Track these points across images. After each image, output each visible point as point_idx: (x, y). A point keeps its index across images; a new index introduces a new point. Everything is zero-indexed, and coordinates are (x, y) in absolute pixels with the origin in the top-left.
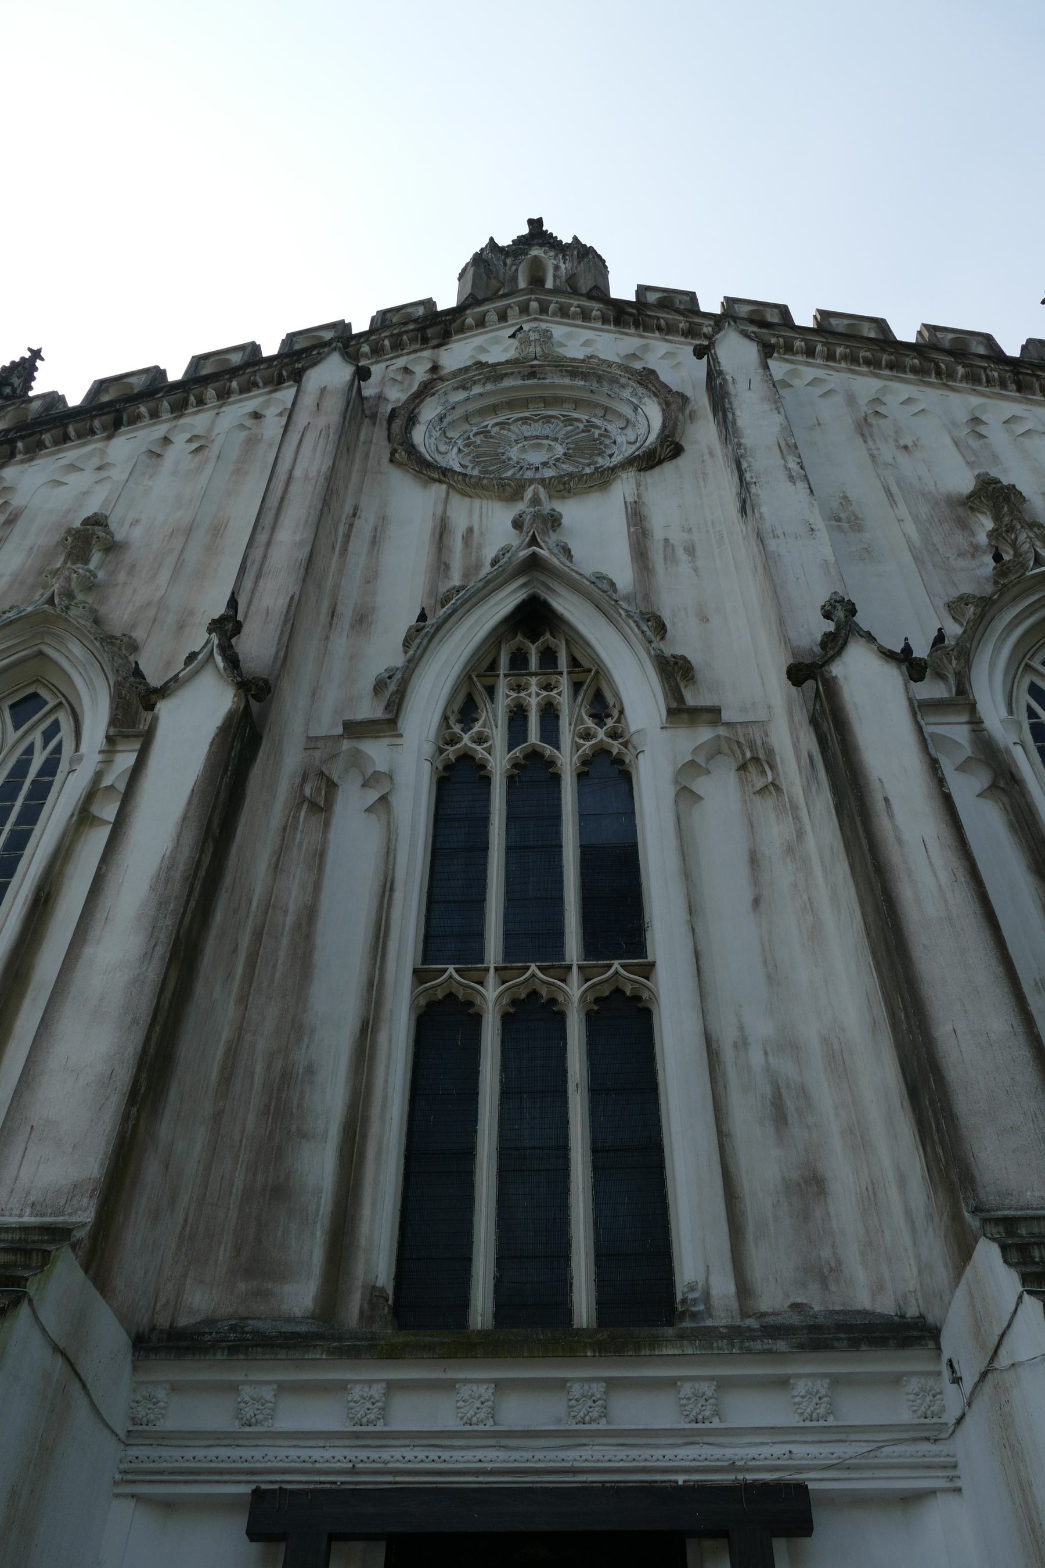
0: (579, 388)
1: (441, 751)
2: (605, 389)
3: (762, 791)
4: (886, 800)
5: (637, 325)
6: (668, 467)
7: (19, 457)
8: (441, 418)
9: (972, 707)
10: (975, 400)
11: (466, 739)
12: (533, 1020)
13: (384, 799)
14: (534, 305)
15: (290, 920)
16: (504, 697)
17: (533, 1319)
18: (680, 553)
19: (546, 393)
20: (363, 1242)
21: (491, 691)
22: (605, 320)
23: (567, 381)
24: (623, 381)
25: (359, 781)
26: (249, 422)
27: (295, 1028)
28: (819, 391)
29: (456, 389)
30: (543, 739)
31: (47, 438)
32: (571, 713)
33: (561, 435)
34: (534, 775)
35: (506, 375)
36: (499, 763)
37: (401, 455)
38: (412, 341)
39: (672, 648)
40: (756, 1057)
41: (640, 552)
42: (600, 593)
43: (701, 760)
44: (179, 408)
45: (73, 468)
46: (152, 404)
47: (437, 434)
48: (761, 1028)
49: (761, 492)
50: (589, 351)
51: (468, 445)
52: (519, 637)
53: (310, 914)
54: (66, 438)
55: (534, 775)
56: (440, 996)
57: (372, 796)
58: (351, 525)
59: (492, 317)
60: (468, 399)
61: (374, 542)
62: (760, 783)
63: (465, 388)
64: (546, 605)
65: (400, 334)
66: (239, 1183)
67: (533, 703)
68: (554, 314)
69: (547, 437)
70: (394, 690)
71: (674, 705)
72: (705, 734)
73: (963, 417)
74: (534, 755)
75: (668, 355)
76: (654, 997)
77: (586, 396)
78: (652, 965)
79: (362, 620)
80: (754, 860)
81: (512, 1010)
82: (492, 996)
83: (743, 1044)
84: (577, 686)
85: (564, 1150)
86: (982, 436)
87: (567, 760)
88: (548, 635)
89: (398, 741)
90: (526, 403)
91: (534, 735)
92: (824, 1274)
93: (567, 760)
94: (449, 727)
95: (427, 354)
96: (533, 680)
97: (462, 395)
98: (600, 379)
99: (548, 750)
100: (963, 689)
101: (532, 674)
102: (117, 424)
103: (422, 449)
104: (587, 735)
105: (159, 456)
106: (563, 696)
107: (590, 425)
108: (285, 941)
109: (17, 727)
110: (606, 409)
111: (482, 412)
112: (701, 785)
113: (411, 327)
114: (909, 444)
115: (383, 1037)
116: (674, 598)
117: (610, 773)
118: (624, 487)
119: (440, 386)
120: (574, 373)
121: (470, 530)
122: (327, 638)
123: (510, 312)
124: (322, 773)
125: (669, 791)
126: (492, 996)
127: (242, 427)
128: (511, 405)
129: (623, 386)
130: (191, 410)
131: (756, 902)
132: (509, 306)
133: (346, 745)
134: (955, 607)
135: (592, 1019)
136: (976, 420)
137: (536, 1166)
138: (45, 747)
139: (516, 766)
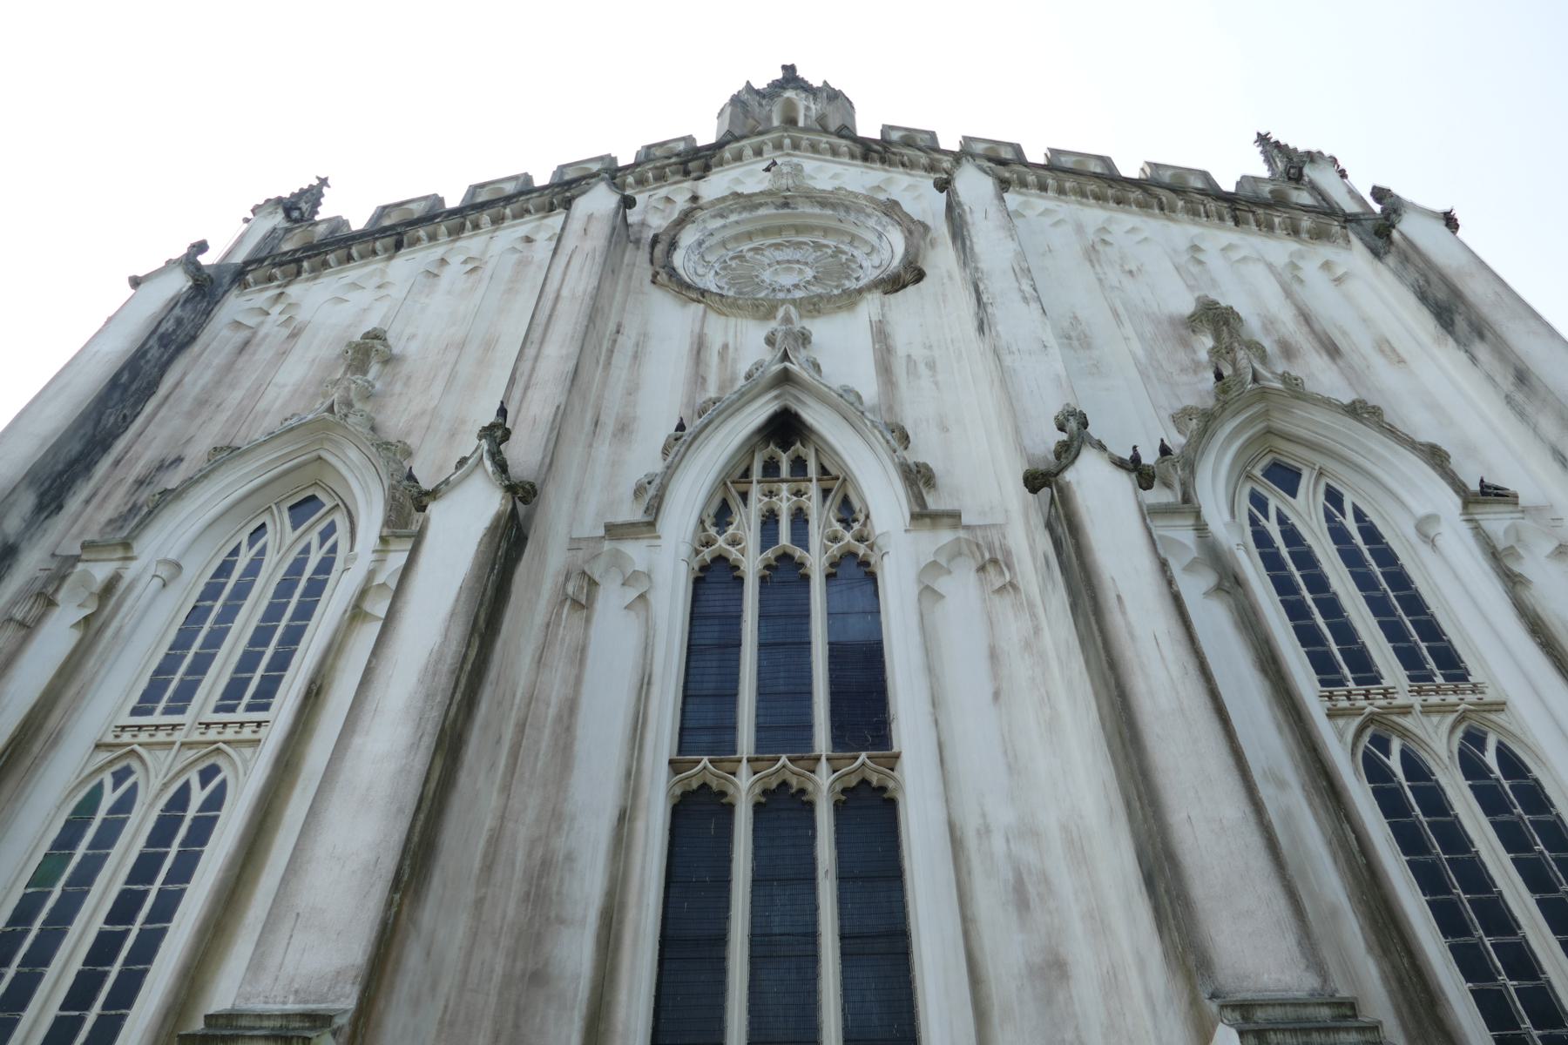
0: (829, 217)
1: (697, 553)
2: (852, 217)
3: (1002, 589)
4: (1119, 597)
5: (883, 161)
6: (911, 289)
7: (304, 276)
8: (700, 244)
9: (1198, 514)
11: (721, 541)
12: (783, 809)
13: (642, 597)
14: (787, 142)
15: (552, 712)
18: (922, 368)
19: (798, 221)
20: (620, 1027)
21: (744, 496)
22: (853, 157)
23: (817, 210)
24: (868, 210)
25: (619, 581)
26: (520, 246)
27: (555, 817)
28: (1048, 221)
29: (714, 217)
30: (793, 541)
31: (331, 258)
32: (819, 519)
33: (810, 260)
34: (785, 575)
35: (761, 205)
36: (752, 564)
37: (663, 277)
38: (674, 173)
39: (916, 455)
40: (998, 844)
41: (885, 369)
42: (847, 405)
43: (943, 561)
44: (456, 232)
45: (355, 286)
46: (430, 228)
47: (695, 258)
48: (1003, 816)
49: (997, 313)
50: (837, 183)
51: (724, 268)
52: (772, 446)
53: (571, 707)
54: (350, 258)
55: (785, 575)
56: (695, 785)
57: (632, 594)
58: (615, 341)
59: (748, 152)
60: (724, 226)
61: (635, 356)
62: (998, 583)
63: (722, 216)
64: (796, 416)
65: (663, 167)
66: (499, 970)
67: (784, 507)
68: (806, 150)
69: (798, 262)
70: (653, 497)
71: (917, 509)
72: (946, 536)
73: (1183, 244)
74: (785, 557)
75: (910, 187)
76: (900, 786)
77: (834, 224)
78: (897, 756)
79: (624, 429)
80: (994, 656)
81: (763, 800)
83: (985, 831)
84: (826, 492)
85: (812, 936)
86: (1200, 262)
87: (816, 562)
88: (798, 444)
89: (656, 542)
90: (779, 230)
94: (704, 530)
95: (688, 184)
96: (784, 486)
97: (719, 222)
98: (847, 209)
99: (798, 552)
100: (1187, 499)
101: (783, 481)
102: (398, 246)
103: (681, 271)
104: (835, 539)
105: (436, 275)
106: (812, 502)
107: (838, 251)
108: (547, 732)
109: (295, 528)
111: (737, 238)
112: (943, 584)
113: (673, 160)
114: (1134, 269)
115: (640, 825)
116: (915, 411)
117: (856, 573)
118: (871, 306)
119: (699, 214)
120: (823, 204)
121: (726, 346)
122: (590, 446)
123: (765, 148)
124: (584, 573)
125: (913, 590)
127: (514, 250)
128: (765, 232)
129: (869, 216)
130: (466, 234)
131: (996, 695)
132: (764, 143)
133: (607, 545)
134: (1180, 418)
135: (839, 808)
136: (1195, 248)
137: (784, 953)
138: (321, 546)
139: (768, 567)
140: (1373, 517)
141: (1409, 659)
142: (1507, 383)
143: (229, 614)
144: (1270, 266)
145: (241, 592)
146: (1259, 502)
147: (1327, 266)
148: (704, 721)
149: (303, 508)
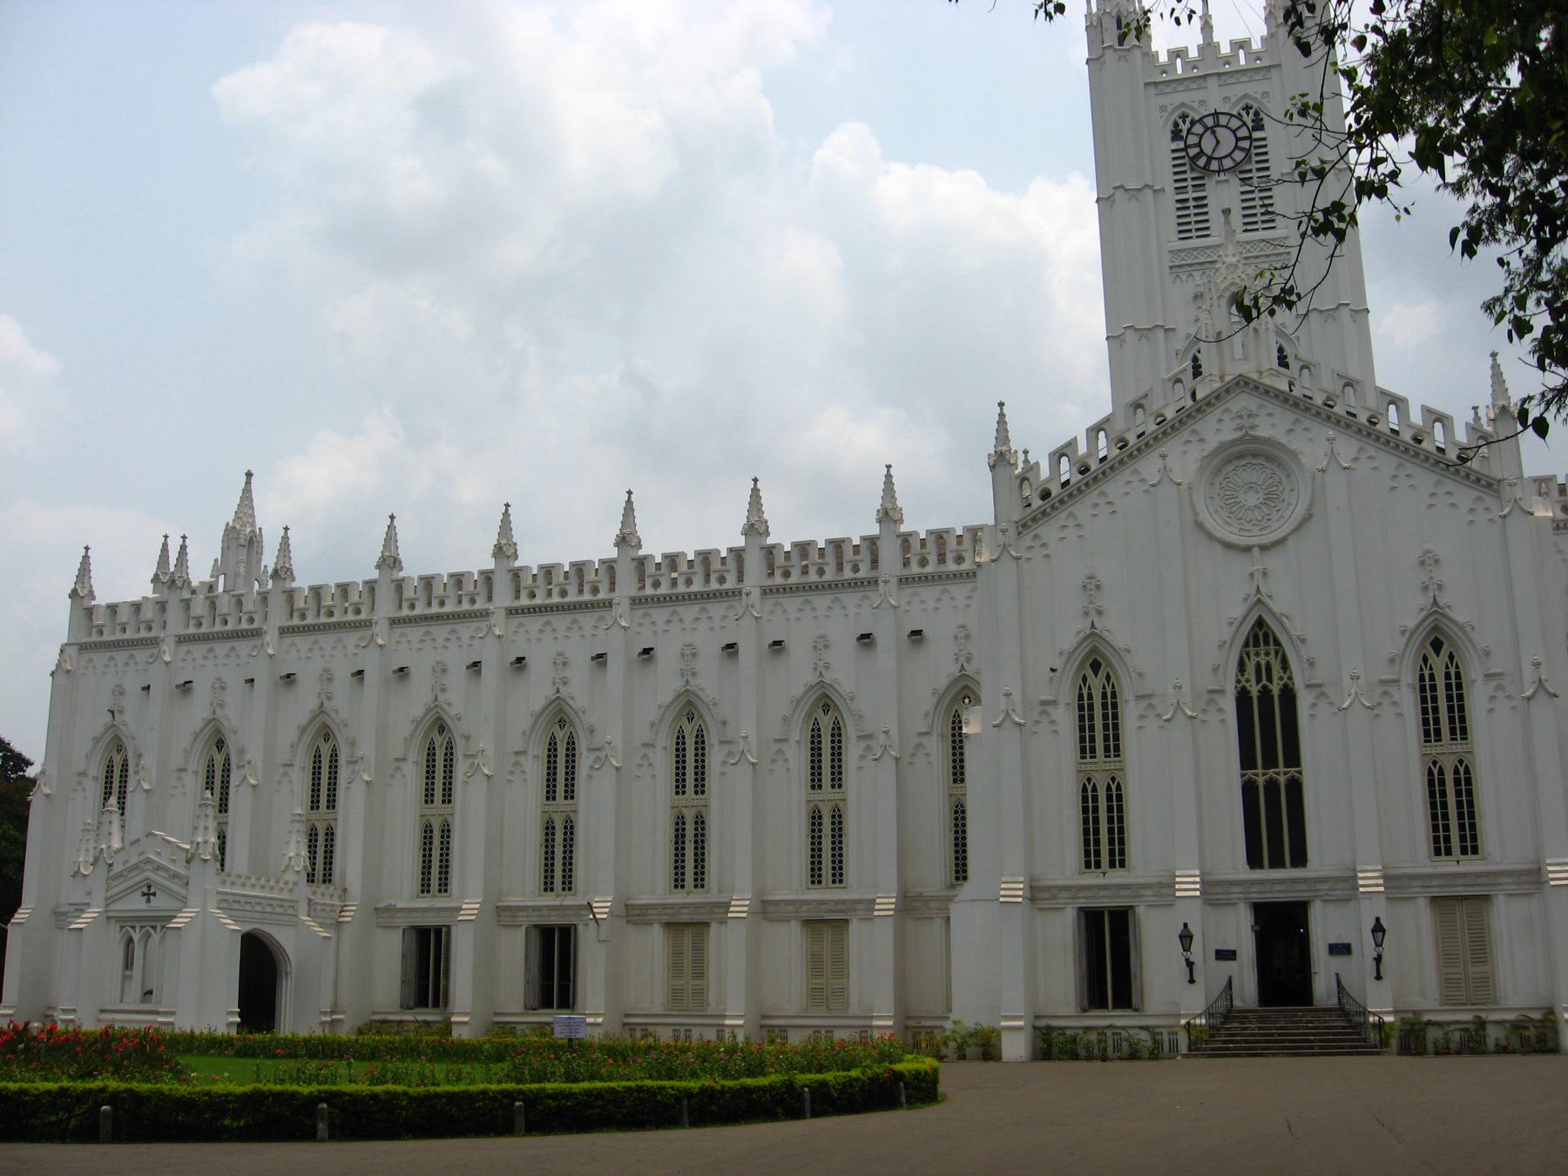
12: (1272, 785)
16: (1254, 659)
17: (1277, 862)
34: (1265, 694)
36: (1254, 690)
45: (1064, 527)
55: (1265, 694)
67: (1263, 663)
74: (1265, 687)
82: (1261, 781)
84: (1277, 653)
87: (1275, 689)
91: (1264, 682)
93: (1275, 689)
106: (1272, 658)
117: (1289, 695)
126: (1261, 781)
141: (1453, 731)
143: (1091, 718)
145: (1091, 707)
146: (1425, 659)
147: (1487, 509)
148: (1247, 761)
149: (1096, 667)
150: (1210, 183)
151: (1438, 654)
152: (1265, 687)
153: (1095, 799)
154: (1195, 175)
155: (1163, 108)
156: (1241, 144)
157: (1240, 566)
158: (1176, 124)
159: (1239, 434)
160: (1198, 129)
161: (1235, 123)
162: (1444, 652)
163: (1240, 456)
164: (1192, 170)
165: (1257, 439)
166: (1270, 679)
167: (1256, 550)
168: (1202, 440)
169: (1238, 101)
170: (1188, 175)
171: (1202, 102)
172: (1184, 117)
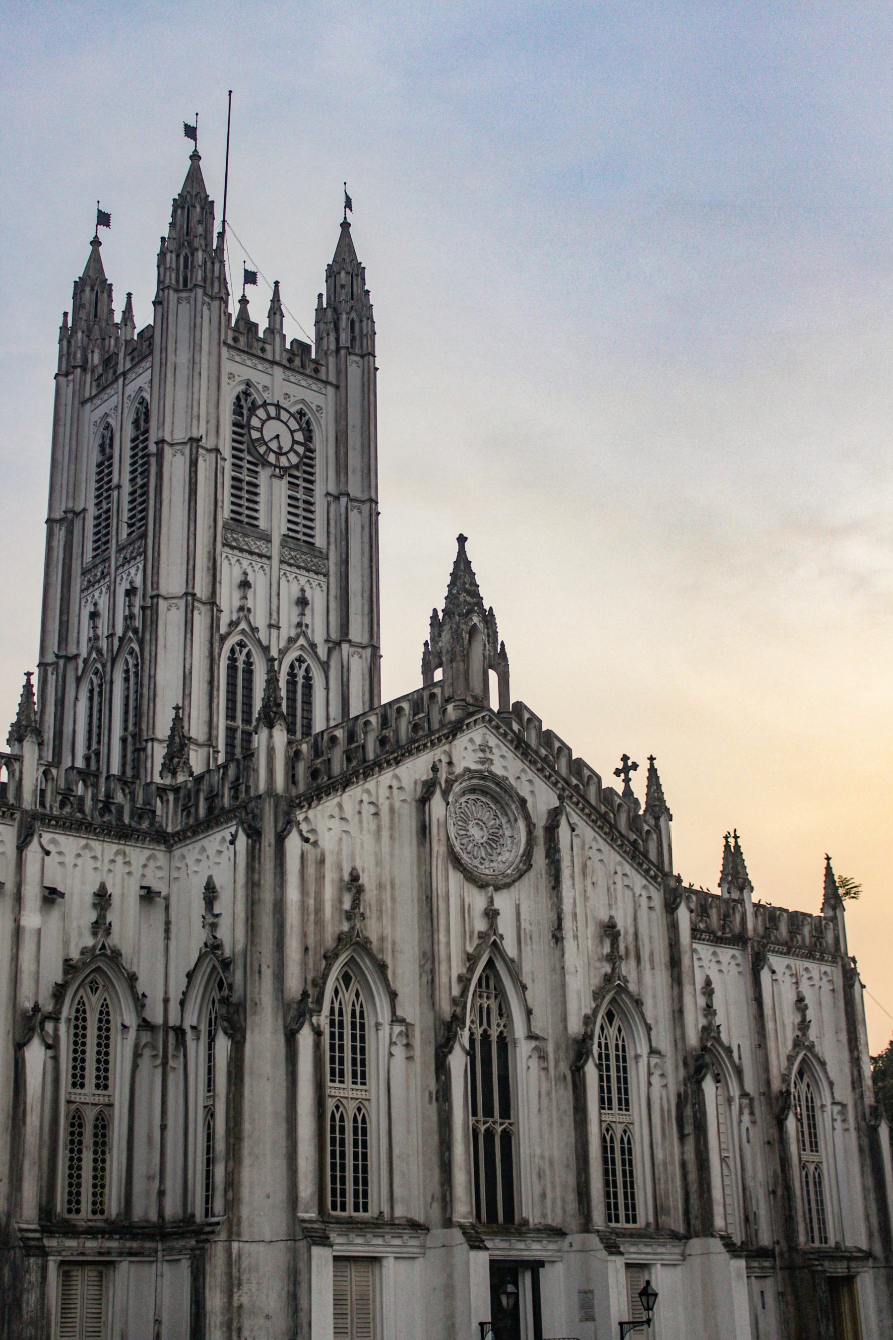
7: (313, 804)
10: (619, 858)
14: (487, 718)
22: (512, 742)
23: (493, 786)
48: (538, 1151)
50: (505, 774)
64: (493, 962)
72: (534, 1044)
73: (612, 872)
92: (544, 1216)
95: (446, 747)
110: (502, 807)
112: (530, 1064)
116: (526, 968)
118: (514, 890)
120: (497, 784)
129: (514, 802)
140: (626, 1043)
142: (677, 1008)
144: (634, 895)
147: (649, 898)
150: (264, 475)
151: (611, 1026)
152: (485, 1031)
153: (342, 1130)
154: (249, 458)
155: (231, 376)
156: (296, 447)
157: (478, 901)
158: (238, 398)
159: (478, 767)
160: (261, 413)
161: (294, 425)
162: (616, 1022)
163: (473, 790)
164: (249, 453)
165: (493, 778)
166: (489, 1025)
167: (491, 888)
168: (450, 763)
169: (296, 403)
170: (245, 455)
171: (265, 387)
172: (246, 394)
